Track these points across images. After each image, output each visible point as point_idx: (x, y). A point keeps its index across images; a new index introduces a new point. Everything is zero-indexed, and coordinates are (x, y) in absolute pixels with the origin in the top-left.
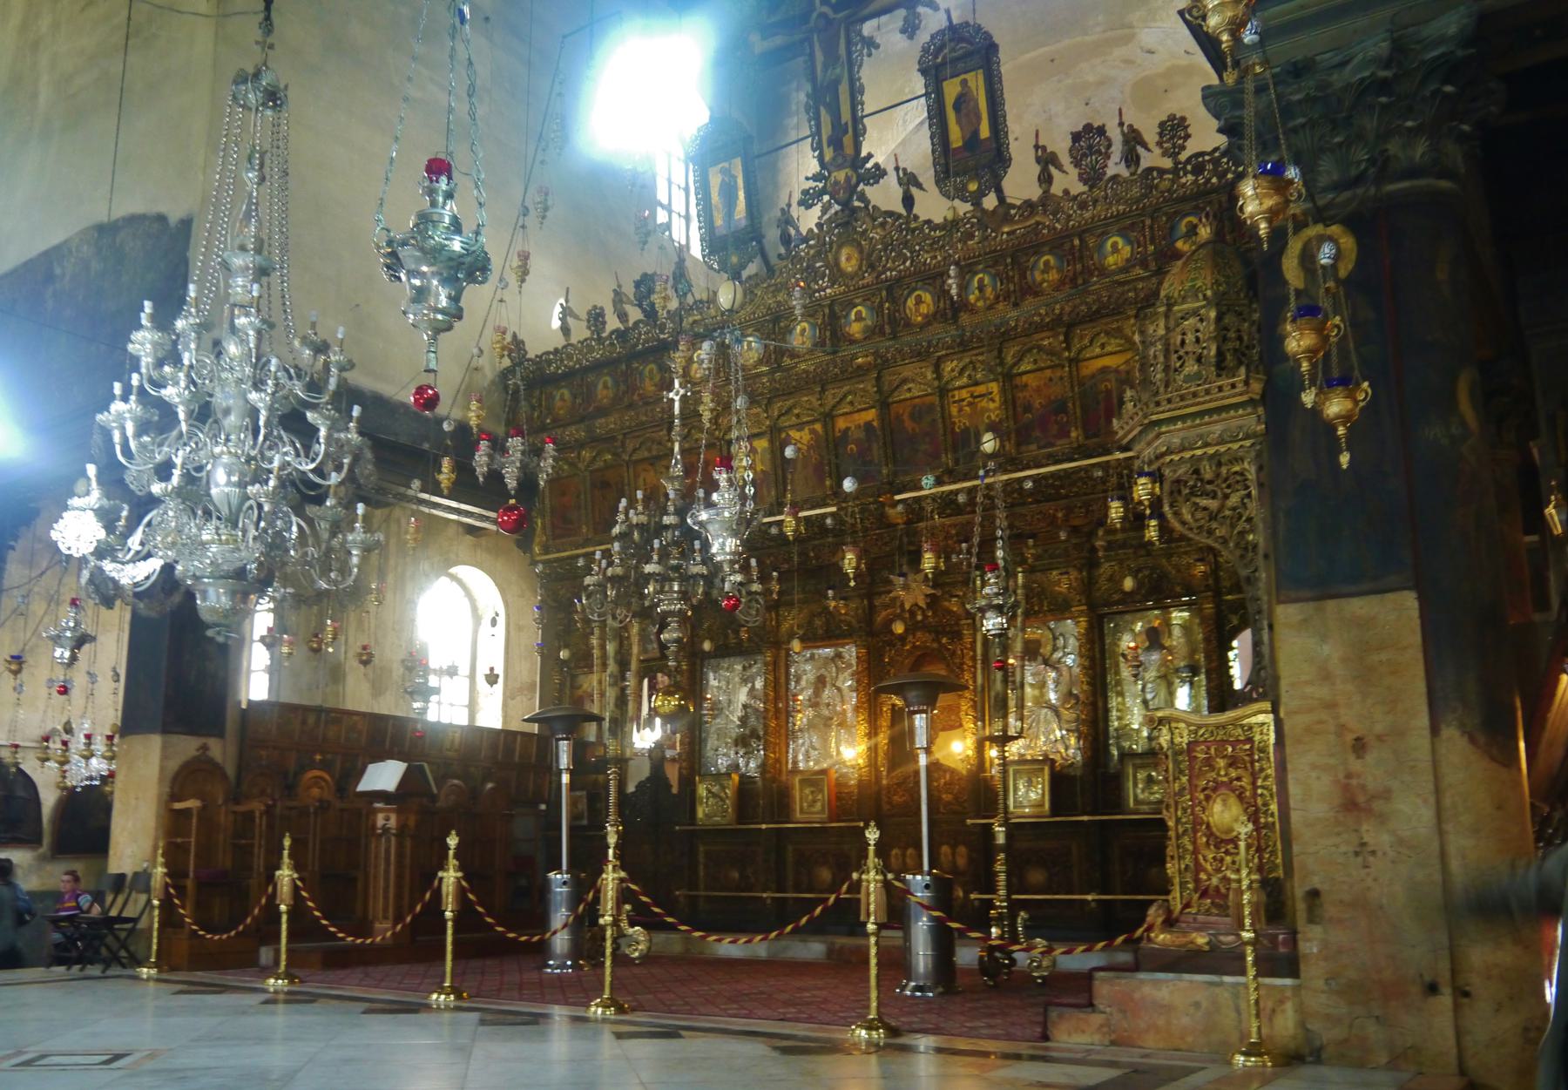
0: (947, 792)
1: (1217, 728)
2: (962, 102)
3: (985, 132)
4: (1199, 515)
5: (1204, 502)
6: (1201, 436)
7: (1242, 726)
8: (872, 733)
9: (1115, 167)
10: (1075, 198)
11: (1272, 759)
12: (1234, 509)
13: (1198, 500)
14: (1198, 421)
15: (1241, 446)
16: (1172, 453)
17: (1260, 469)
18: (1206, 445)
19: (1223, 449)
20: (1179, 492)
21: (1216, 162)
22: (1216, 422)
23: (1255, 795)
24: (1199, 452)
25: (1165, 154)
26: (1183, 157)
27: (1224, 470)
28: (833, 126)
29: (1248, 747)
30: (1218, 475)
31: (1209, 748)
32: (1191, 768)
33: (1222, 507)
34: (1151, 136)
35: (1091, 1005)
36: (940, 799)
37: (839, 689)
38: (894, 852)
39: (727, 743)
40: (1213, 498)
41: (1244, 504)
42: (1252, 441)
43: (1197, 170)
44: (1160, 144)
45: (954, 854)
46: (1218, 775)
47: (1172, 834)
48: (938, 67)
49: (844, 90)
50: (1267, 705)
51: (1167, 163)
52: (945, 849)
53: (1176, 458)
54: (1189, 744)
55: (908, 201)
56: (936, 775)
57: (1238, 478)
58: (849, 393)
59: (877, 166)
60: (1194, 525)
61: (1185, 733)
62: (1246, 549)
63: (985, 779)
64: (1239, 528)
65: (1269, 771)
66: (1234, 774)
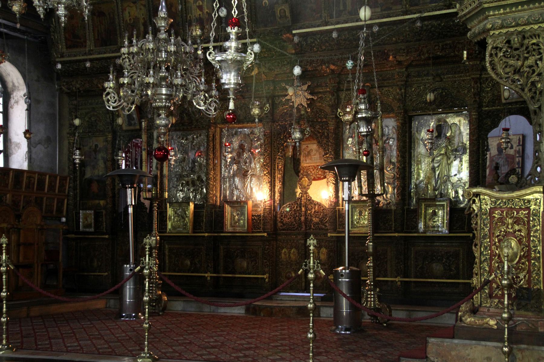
0: (316, 217)
1: (509, 200)
4: (508, 70)
5: (511, 62)
7: (524, 200)
11: (541, 220)
12: (530, 67)
13: (508, 60)
14: (514, 9)
15: (540, 27)
16: (494, 30)
18: (517, 25)
19: (528, 28)
20: (496, 54)
22: (525, 10)
23: (529, 240)
24: (512, 29)
27: (526, 41)
29: (526, 212)
30: (522, 45)
31: (502, 212)
32: (491, 223)
36: (311, 220)
37: (252, 153)
38: (284, 251)
39: (182, 184)
40: (518, 60)
41: (537, 64)
45: (319, 253)
46: (507, 227)
47: (477, 260)
54: (491, 208)
56: (310, 207)
57: (534, 47)
61: (489, 203)
62: (535, 93)
63: (339, 210)
64: (532, 80)
65: (538, 227)
66: (517, 228)
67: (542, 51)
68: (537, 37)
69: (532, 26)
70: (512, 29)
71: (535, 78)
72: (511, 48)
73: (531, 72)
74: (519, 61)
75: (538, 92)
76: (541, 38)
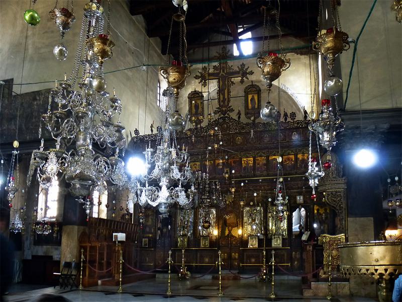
2: (253, 99)
3: (256, 106)
6: (335, 187)
8: (218, 228)
9: (282, 119)
10: (274, 124)
17: (344, 194)
21: (301, 123)
25: (292, 119)
26: (295, 120)
34: (289, 115)
35: (311, 288)
43: (298, 124)
44: (290, 117)
49: (226, 91)
50: (344, 234)
51: (292, 121)
52: (233, 254)
55: (239, 118)
59: (232, 109)
71: (340, 203)
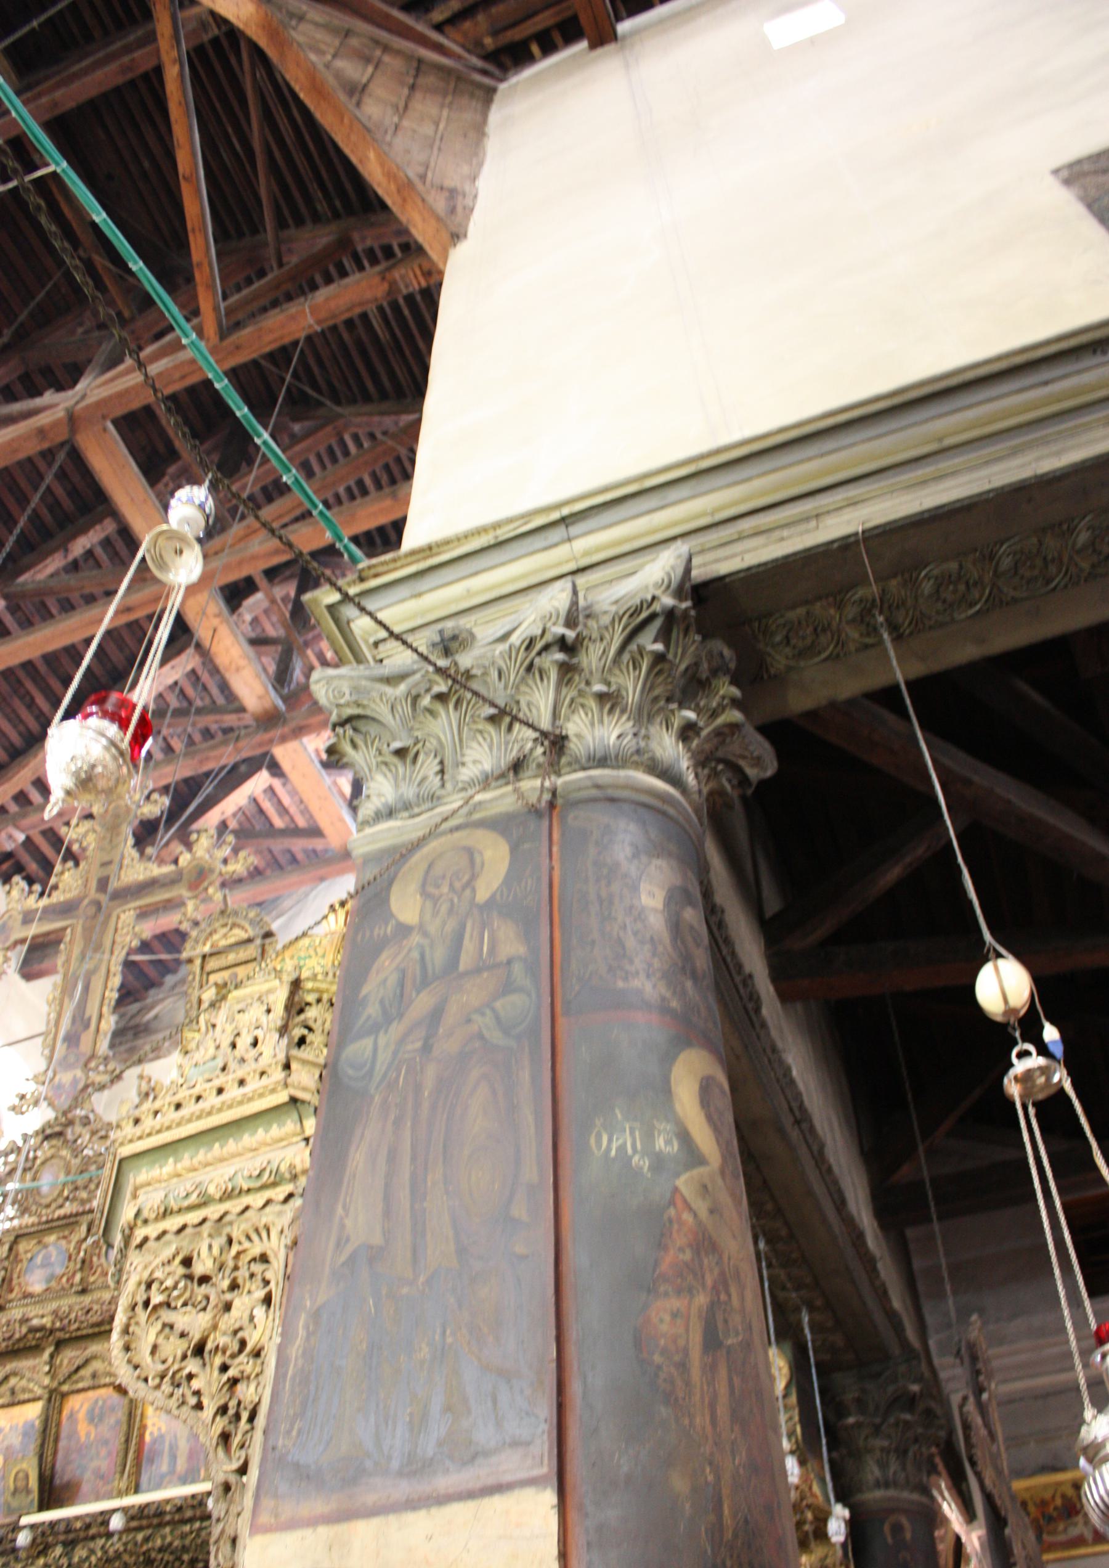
15: (268, 1202)
16: (146, 1222)
18: (205, 1202)
19: (234, 1206)
20: (147, 1303)
24: (193, 1217)
28: (74, 1020)
33: (215, 1327)
41: (252, 1318)
42: (288, 1188)
48: (204, 957)
53: (152, 1231)
57: (257, 1268)
58: (14, 1373)
60: (152, 1367)
62: (237, 1416)
64: (231, 1373)
67: (269, 1275)
68: (264, 1234)
69: (246, 1200)
70: (193, 1217)
72: (189, 1277)
73: (236, 1347)
74: (202, 1314)
75: (245, 1416)
76: (274, 1234)
